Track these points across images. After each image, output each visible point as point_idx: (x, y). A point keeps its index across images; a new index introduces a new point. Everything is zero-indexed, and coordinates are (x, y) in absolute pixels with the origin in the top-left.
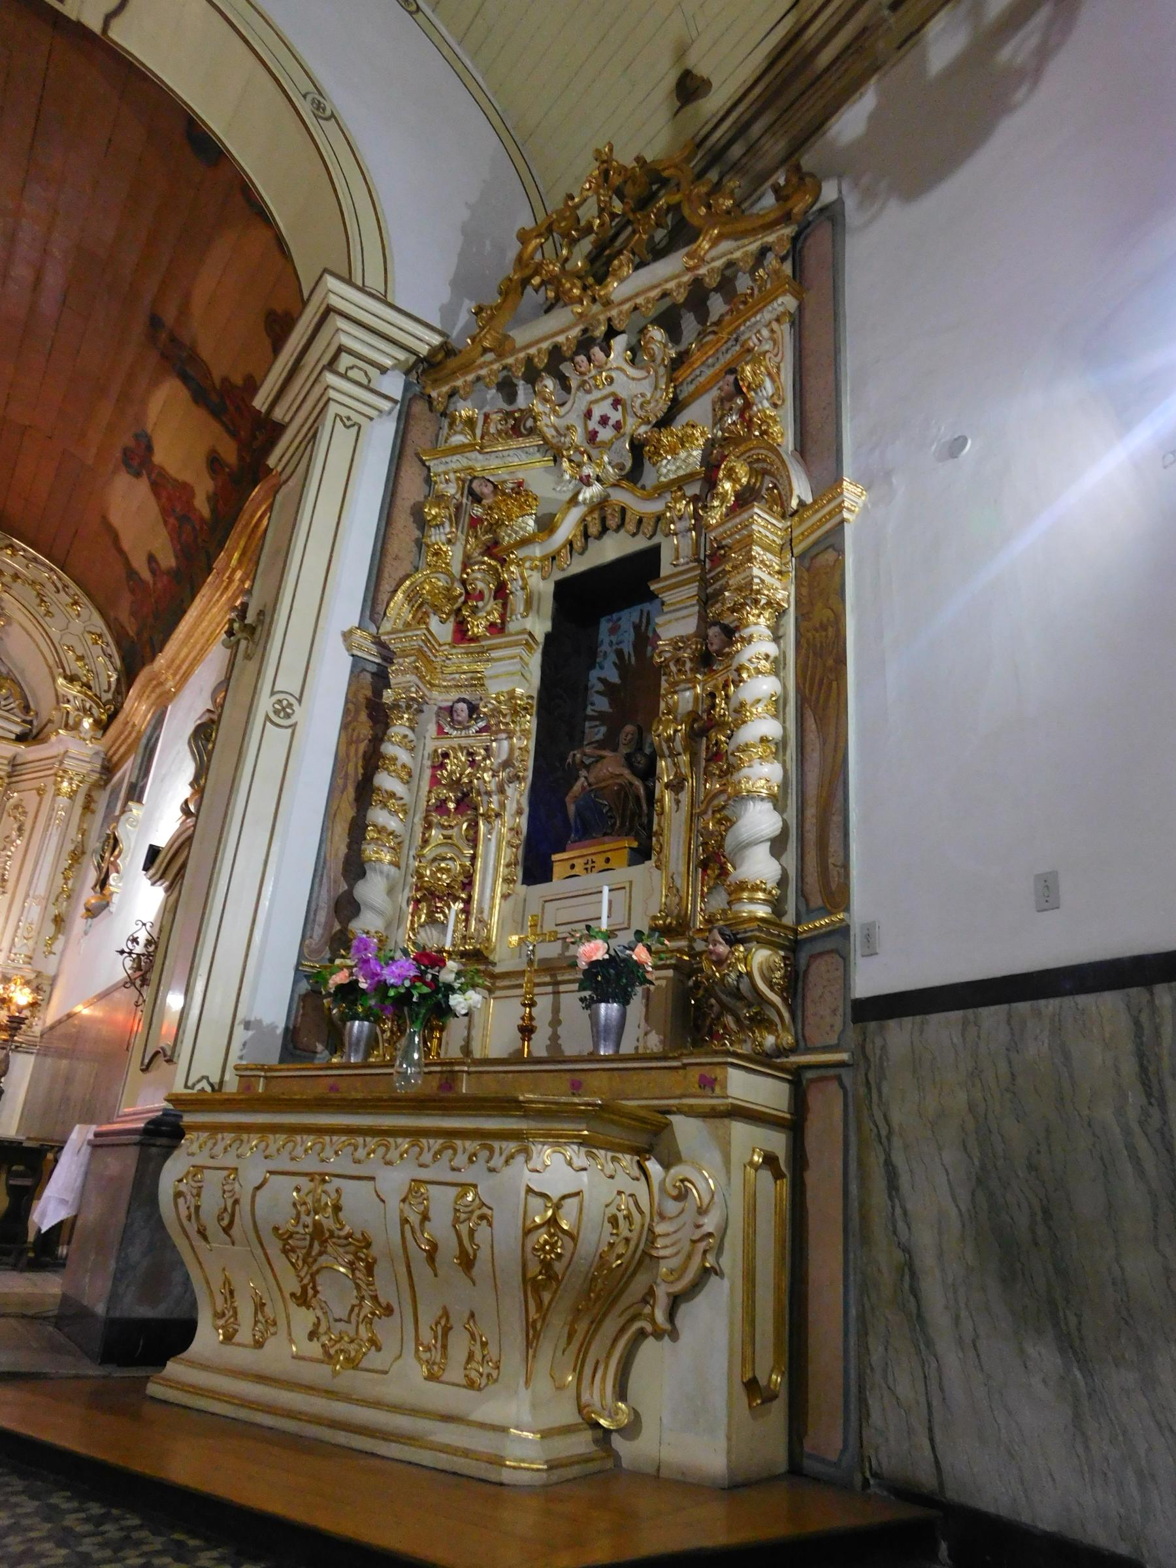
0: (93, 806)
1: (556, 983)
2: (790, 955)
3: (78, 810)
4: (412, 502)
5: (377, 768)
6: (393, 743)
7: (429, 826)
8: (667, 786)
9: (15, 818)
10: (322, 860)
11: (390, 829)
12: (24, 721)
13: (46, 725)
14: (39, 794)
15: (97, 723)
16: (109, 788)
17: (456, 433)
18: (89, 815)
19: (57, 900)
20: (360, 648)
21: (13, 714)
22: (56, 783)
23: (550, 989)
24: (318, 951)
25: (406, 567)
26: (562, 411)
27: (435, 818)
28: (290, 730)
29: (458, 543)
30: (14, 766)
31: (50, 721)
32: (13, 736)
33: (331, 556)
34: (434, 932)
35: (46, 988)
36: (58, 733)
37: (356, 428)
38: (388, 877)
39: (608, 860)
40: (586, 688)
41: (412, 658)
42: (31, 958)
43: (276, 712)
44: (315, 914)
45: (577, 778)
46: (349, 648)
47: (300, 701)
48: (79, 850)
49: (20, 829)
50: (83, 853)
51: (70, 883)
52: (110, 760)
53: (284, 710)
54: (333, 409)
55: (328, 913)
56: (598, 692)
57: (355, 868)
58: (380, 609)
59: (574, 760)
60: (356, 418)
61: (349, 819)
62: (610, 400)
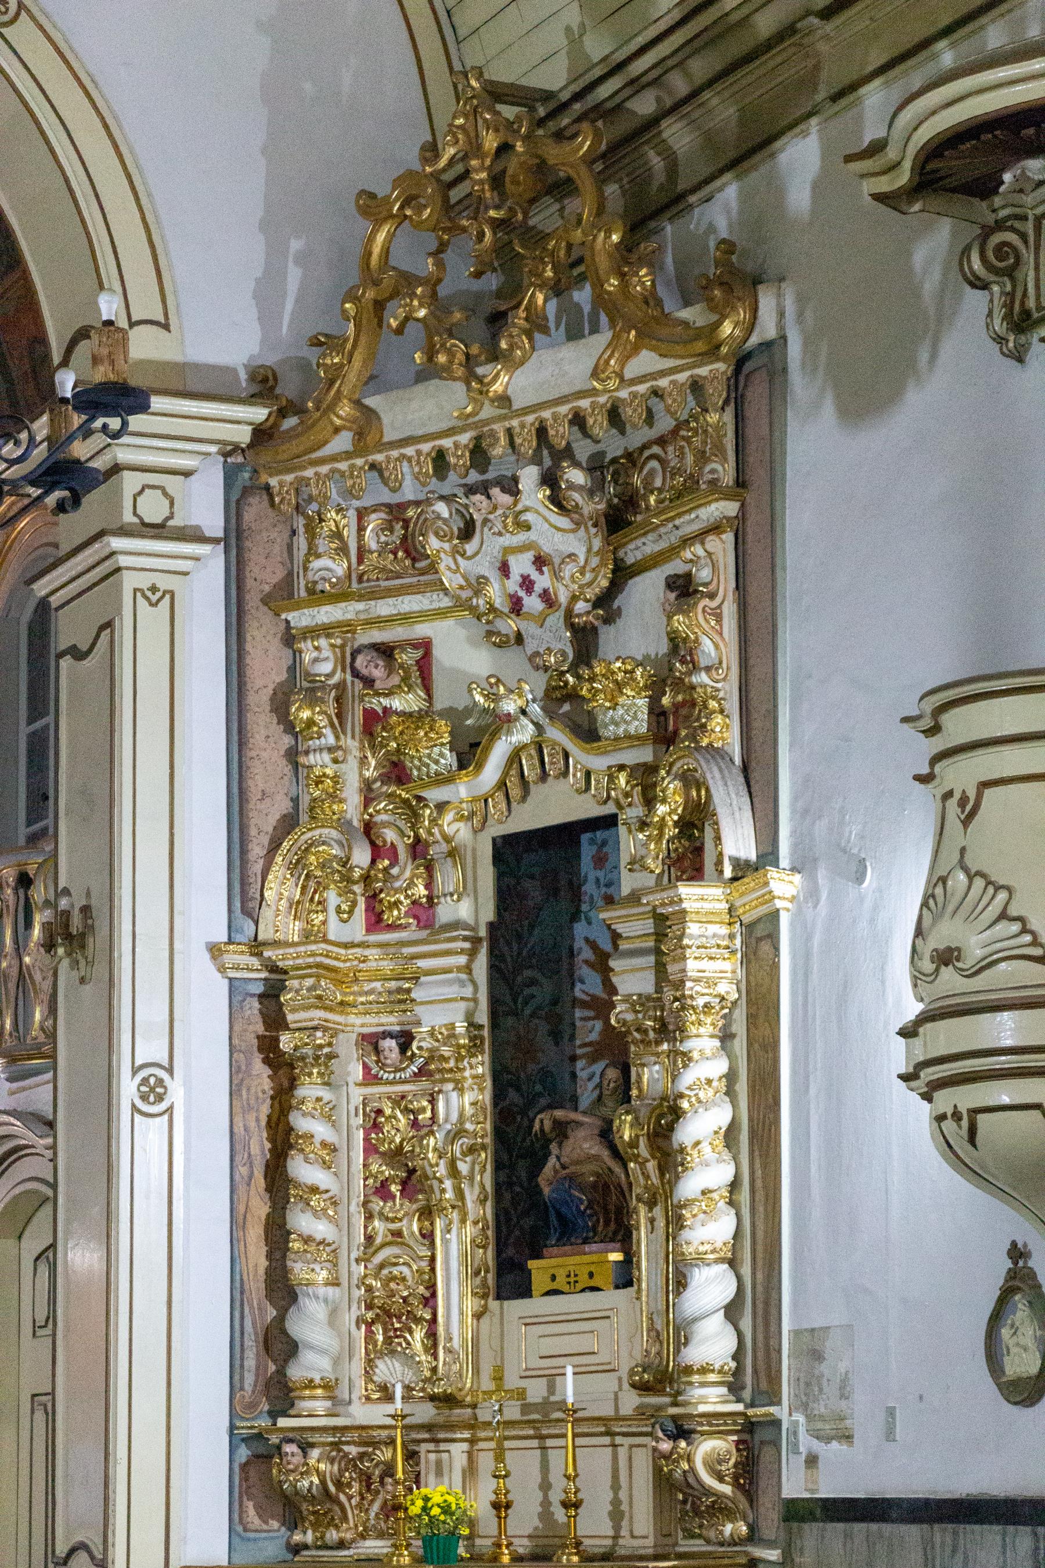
1: (542, 1438)
2: (746, 1436)
4: (272, 686)
5: (291, 1147)
6: (304, 1115)
7: (369, 1217)
8: (639, 1199)
10: (238, 1285)
11: (319, 1237)
17: (318, 556)
20: (237, 968)
23: (535, 1443)
24: (252, 1406)
25: (281, 806)
26: (470, 548)
27: (377, 1204)
28: (166, 1117)
29: (350, 758)
33: (172, 835)
34: (397, 1364)
37: (168, 596)
38: (326, 1301)
39: (591, 1275)
40: (572, 954)
41: (309, 982)
43: (144, 1098)
44: (242, 1359)
45: (547, 1155)
46: (222, 969)
47: (170, 1070)
53: (153, 1091)
54: (130, 581)
55: (258, 1354)
56: (586, 962)
57: (282, 1290)
58: (254, 891)
59: (542, 1130)
60: (164, 582)
61: (263, 1218)
62: (529, 556)
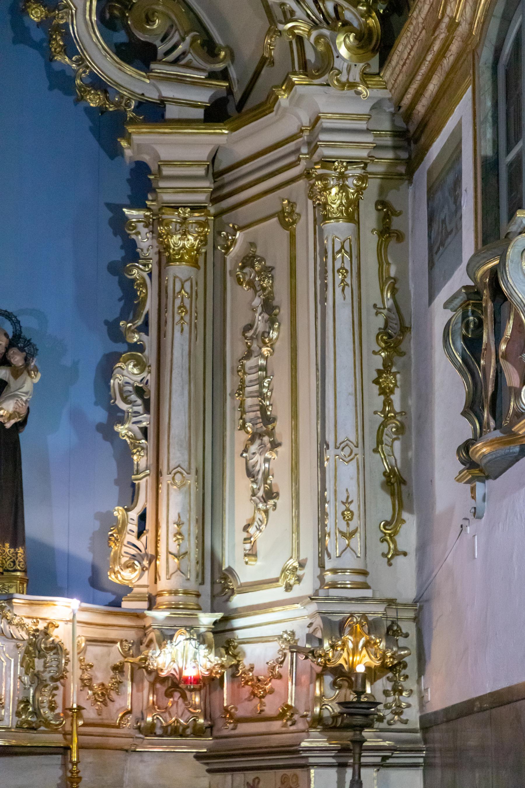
0: (396, 223)
3: (370, 241)
9: (251, 284)
12: (212, 75)
13: (257, 74)
14: (285, 225)
15: (363, 39)
16: (421, 175)
18: (393, 242)
19: (380, 442)
21: (188, 66)
22: (311, 194)
30: (217, 175)
31: (263, 61)
32: (199, 114)
35: (408, 627)
36: (291, 86)
42: (364, 573)
48: (395, 325)
49: (269, 306)
50: (404, 329)
51: (396, 398)
52: (408, 116)
